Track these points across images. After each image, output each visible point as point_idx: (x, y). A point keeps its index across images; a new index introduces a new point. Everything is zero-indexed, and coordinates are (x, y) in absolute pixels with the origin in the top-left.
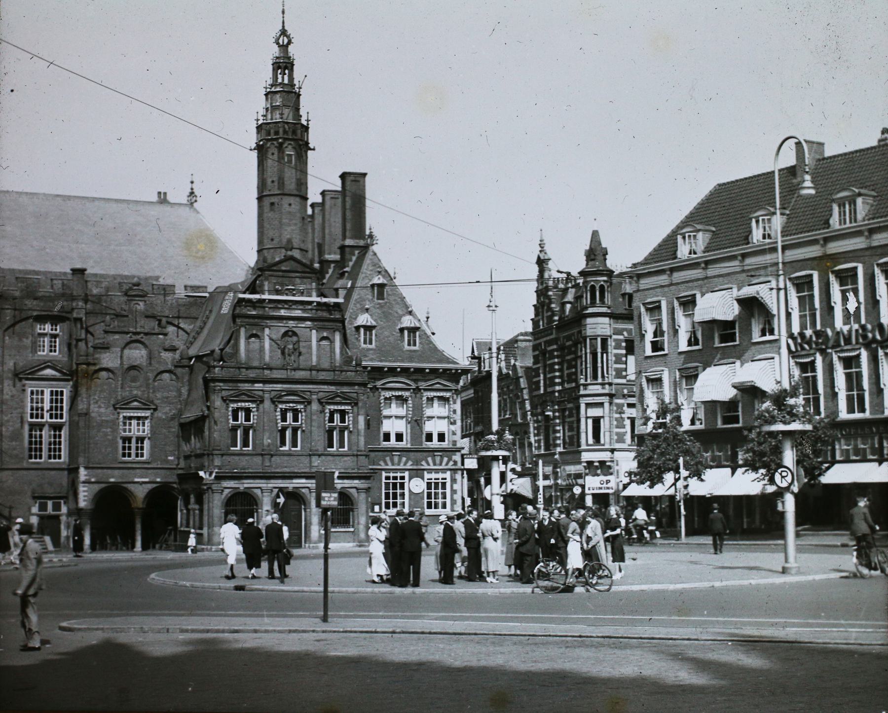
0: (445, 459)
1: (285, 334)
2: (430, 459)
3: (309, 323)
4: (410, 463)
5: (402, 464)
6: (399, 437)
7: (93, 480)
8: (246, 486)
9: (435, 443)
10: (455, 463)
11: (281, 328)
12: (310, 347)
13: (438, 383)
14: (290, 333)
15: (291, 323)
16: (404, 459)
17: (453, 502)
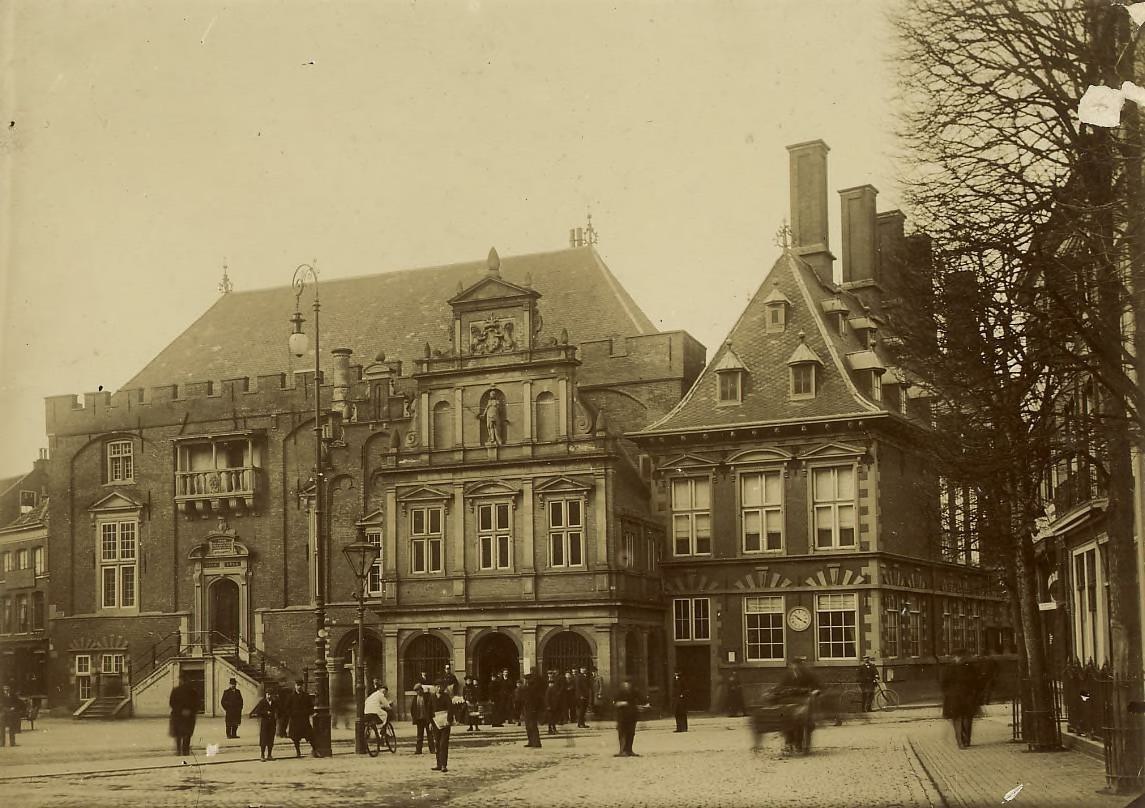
0: (849, 573)
1: (486, 396)
2: (821, 575)
3: (517, 376)
4: (788, 582)
5: (773, 585)
6: (773, 540)
7: (334, 622)
8: (431, 626)
9: (835, 546)
10: (867, 579)
11: (478, 387)
12: (522, 413)
13: (831, 448)
14: (491, 394)
15: (493, 379)
16: (776, 577)
17: (865, 645)
